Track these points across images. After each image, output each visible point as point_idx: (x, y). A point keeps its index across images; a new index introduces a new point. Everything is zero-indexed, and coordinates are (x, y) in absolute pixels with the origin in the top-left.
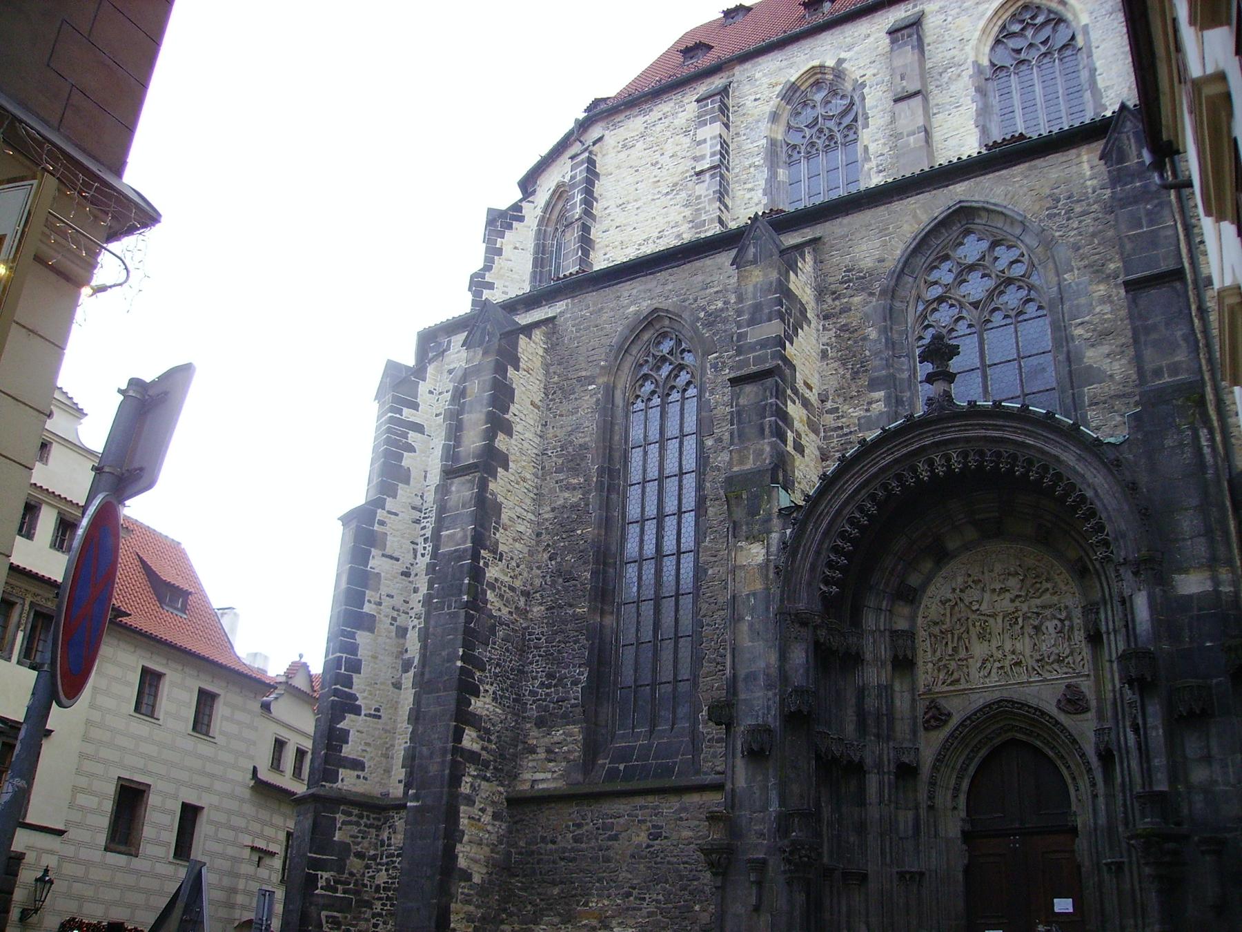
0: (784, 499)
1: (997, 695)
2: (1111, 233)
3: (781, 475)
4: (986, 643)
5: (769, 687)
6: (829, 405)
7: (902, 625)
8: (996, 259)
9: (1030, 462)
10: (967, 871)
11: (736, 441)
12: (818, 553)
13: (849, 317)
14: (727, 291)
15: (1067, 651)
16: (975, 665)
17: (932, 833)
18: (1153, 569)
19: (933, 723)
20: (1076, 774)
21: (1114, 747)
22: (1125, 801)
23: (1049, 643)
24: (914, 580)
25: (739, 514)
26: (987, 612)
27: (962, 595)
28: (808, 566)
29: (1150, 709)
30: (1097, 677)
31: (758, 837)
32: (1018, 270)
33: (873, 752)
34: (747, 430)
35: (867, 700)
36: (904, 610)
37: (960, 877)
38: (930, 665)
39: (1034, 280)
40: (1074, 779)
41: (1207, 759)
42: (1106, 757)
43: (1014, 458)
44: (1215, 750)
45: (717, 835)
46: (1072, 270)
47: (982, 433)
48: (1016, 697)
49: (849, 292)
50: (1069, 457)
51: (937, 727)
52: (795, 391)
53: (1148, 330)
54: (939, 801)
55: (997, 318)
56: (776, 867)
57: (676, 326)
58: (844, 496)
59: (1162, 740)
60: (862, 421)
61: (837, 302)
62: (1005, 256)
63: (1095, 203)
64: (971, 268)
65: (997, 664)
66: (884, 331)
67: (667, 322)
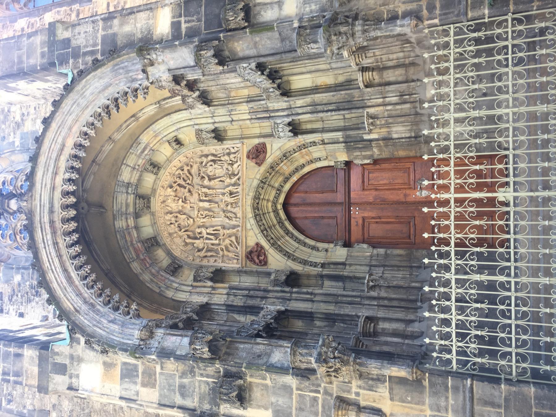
10: (374, 247)
11: (20, 379)
17: (342, 266)
19: (262, 258)
20: (308, 158)
30: (243, 138)
46: (14, 142)
48: (252, 194)
51: (265, 254)
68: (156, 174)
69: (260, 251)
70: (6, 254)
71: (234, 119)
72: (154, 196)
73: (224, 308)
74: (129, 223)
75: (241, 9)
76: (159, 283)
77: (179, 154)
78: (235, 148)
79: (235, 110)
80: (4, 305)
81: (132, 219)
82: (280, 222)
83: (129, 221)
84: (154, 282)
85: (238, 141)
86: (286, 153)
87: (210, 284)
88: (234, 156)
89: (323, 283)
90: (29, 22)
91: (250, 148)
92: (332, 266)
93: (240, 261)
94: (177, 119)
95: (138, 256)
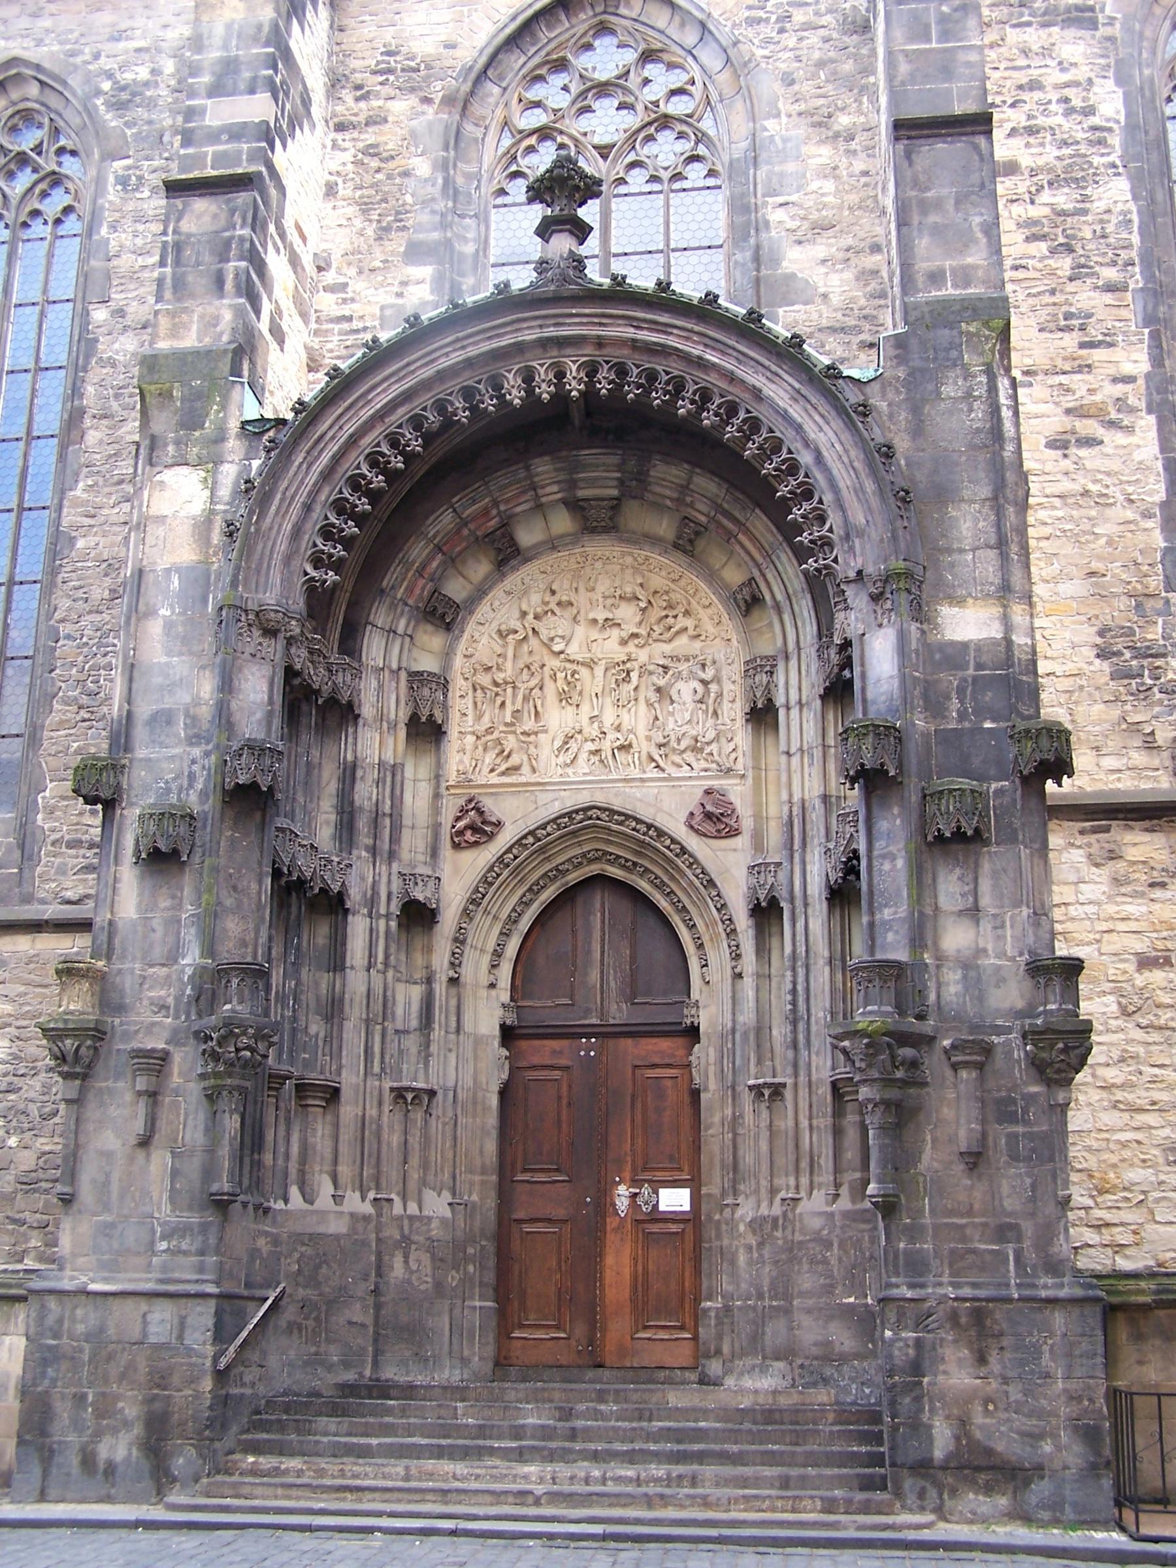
0: (252, 411)
1: (583, 798)
2: (848, 67)
3: (246, 366)
4: (570, 710)
5: (194, 739)
6: (330, 277)
7: (427, 663)
8: (646, 81)
9: (705, 396)
10: (504, 1093)
11: (168, 294)
12: (308, 508)
13: (381, 133)
14: (159, 50)
15: (711, 735)
16: (546, 747)
17: (453, 1024)
18: (909, 591)
19: (468, 836)
20: (706, 939)
21: (782, 894)
22: (794, 983)
23: (683, 716)
24: (456, 589)
25: (163, 423)
26: (579, 657)
27: (537, 625)
28: (288, 527)
29: (883, 825)
31: (154, 1009)
32: (678, 107)
33: (361, 877)
34: (190, 278)
35: (359, 786)
36: (432, 639)
37: (494, 1101)
38: (470, 739)
39: (707, 125)
40: (700, 947)
41: (973, 912)
42: (766, 912)
43: (679, 386)
44: (985, 901)
45: (77, 1003)
46: (778, 115)
47: (630, 332)
49: (386, 90)
50: (779, 391)
52: (282, 235)
53: (925, 207)
54: (467, 972)
55: (637, 180)
56: (185, 1068)
57: (53, 101)
58: (367, 413)
59: (902, 879)
60: (388, 312)
61: (363, 105)
62: (661, 79)
63: (830, 11)
64: (603, 89)
66: (444, 166)
67: (34, 90)
68: (676, 546)
69: (485, 832)
70: (485, 111)
71: (795, 760)
73: (350, 757)
74: (549, 490)
75: (959, 828)
78: (733, 755)
79: (811, 765)
80: (356, 134)
81: (559, 496)
82: (560, 872)
83: (555, 488)
85: (750, 764)
86: (714, 886)
87: (404, 715)
89: (415, 983)
90: (1110, 130)
92: (453, 1002)
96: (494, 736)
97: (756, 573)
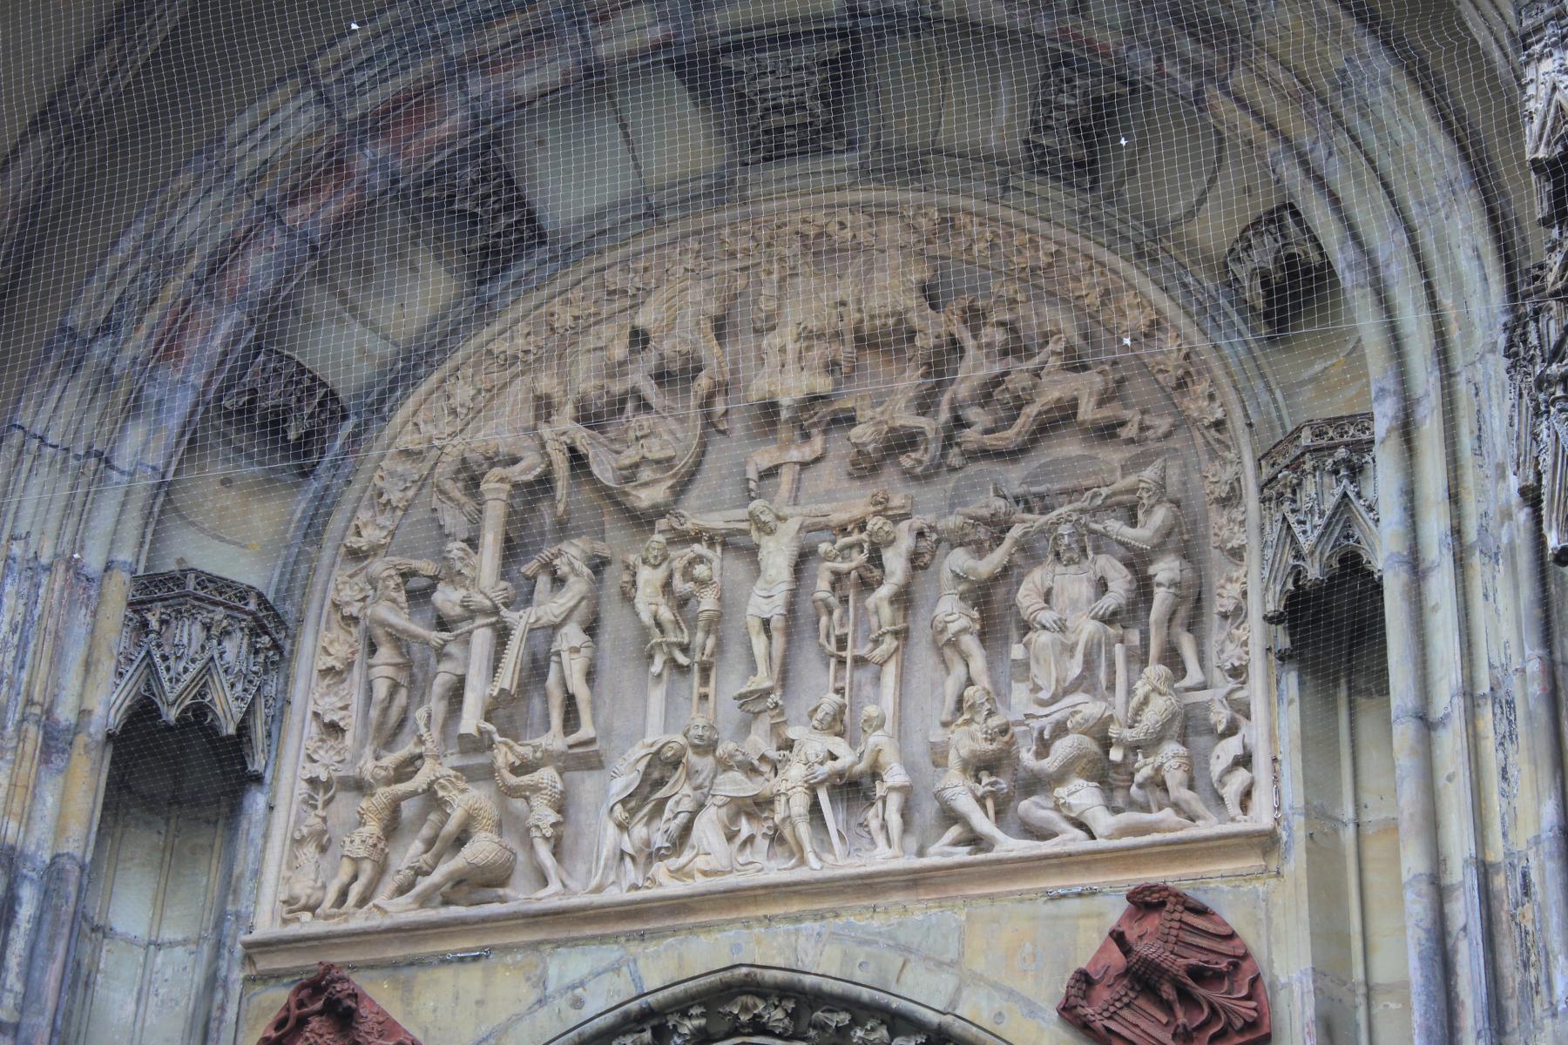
1: (703, 954)
24: (342, 351)
65: (735, 785)
68: (1040, 162)
72: (866, 173)
76: (153, 316)
77: (1204, 313)
78: (1240, 777)
81: (657, 33)
84: (164, 278)
85: (1293, 793)
87: (106, 704)
88: (1175, 778)
91: (1233, 915)
93: (307, 925)
94: (1441, 241)
95: (374, 126)
96: (419, 781)
97: (1292, 174)
